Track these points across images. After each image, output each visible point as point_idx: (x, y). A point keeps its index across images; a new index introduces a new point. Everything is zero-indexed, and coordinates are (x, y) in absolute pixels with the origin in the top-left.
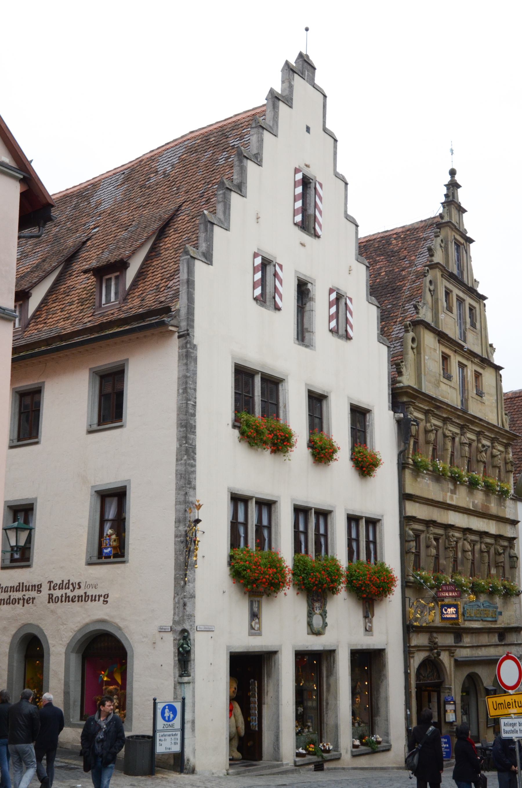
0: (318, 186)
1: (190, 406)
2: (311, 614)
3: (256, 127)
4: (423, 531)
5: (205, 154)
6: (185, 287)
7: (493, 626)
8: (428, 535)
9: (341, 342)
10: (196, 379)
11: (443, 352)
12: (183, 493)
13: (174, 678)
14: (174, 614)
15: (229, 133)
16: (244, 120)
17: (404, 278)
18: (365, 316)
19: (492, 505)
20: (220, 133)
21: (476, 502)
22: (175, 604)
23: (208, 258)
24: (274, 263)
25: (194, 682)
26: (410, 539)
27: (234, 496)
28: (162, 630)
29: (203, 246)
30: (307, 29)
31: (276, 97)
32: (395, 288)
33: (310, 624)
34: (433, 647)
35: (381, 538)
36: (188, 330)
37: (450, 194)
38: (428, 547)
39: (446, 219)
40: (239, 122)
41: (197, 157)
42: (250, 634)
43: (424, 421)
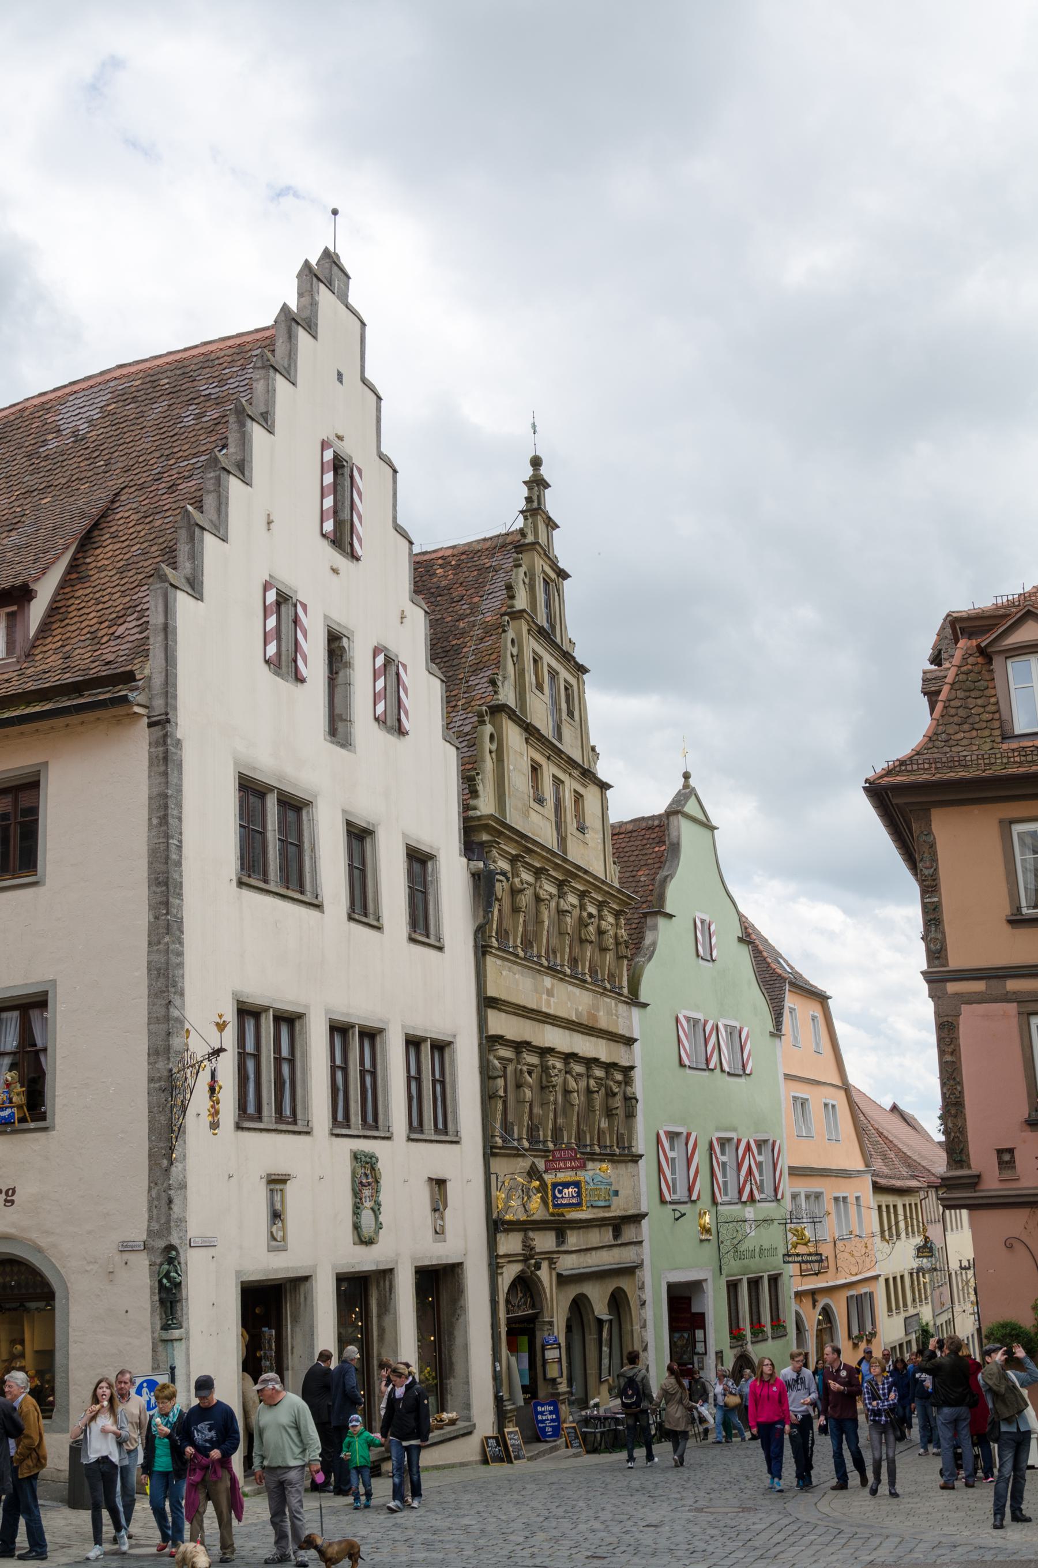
0: (356, 473)
1: (173, 848)
2: (358, 1208)
3: (263, 368)
4: (510, 1060)
5: (154, 406)
6: (160, 638)
7: (607, 1215)
8: (519, 1067)
9: (392, 739)
10: (181, 800)
11: (532, 760)
12: (164, 1002)
13: (153, 1332)
14: (150, 1218)
15: (196, 374)
16: (223, 353)
17: (463, 633)
18: (424, 693)
19: (601, 1013)
20: (178, 372)
21: (580, 1008)
23: (195, 587)
24: (294, 600)
25: (188, 1338)
26: (496, 1074)
28: (126, 1248)
29: (186, 567)
31: (294, 319)
32: (448, 649)
33: (356, 1227)
34: (528, 1255)
35: (453, 1074)
36: (167, 714)
37: (535, 498)
39: (530, 538)
40: (213, 356)
41: (138, 410)
42: (270, 1250)
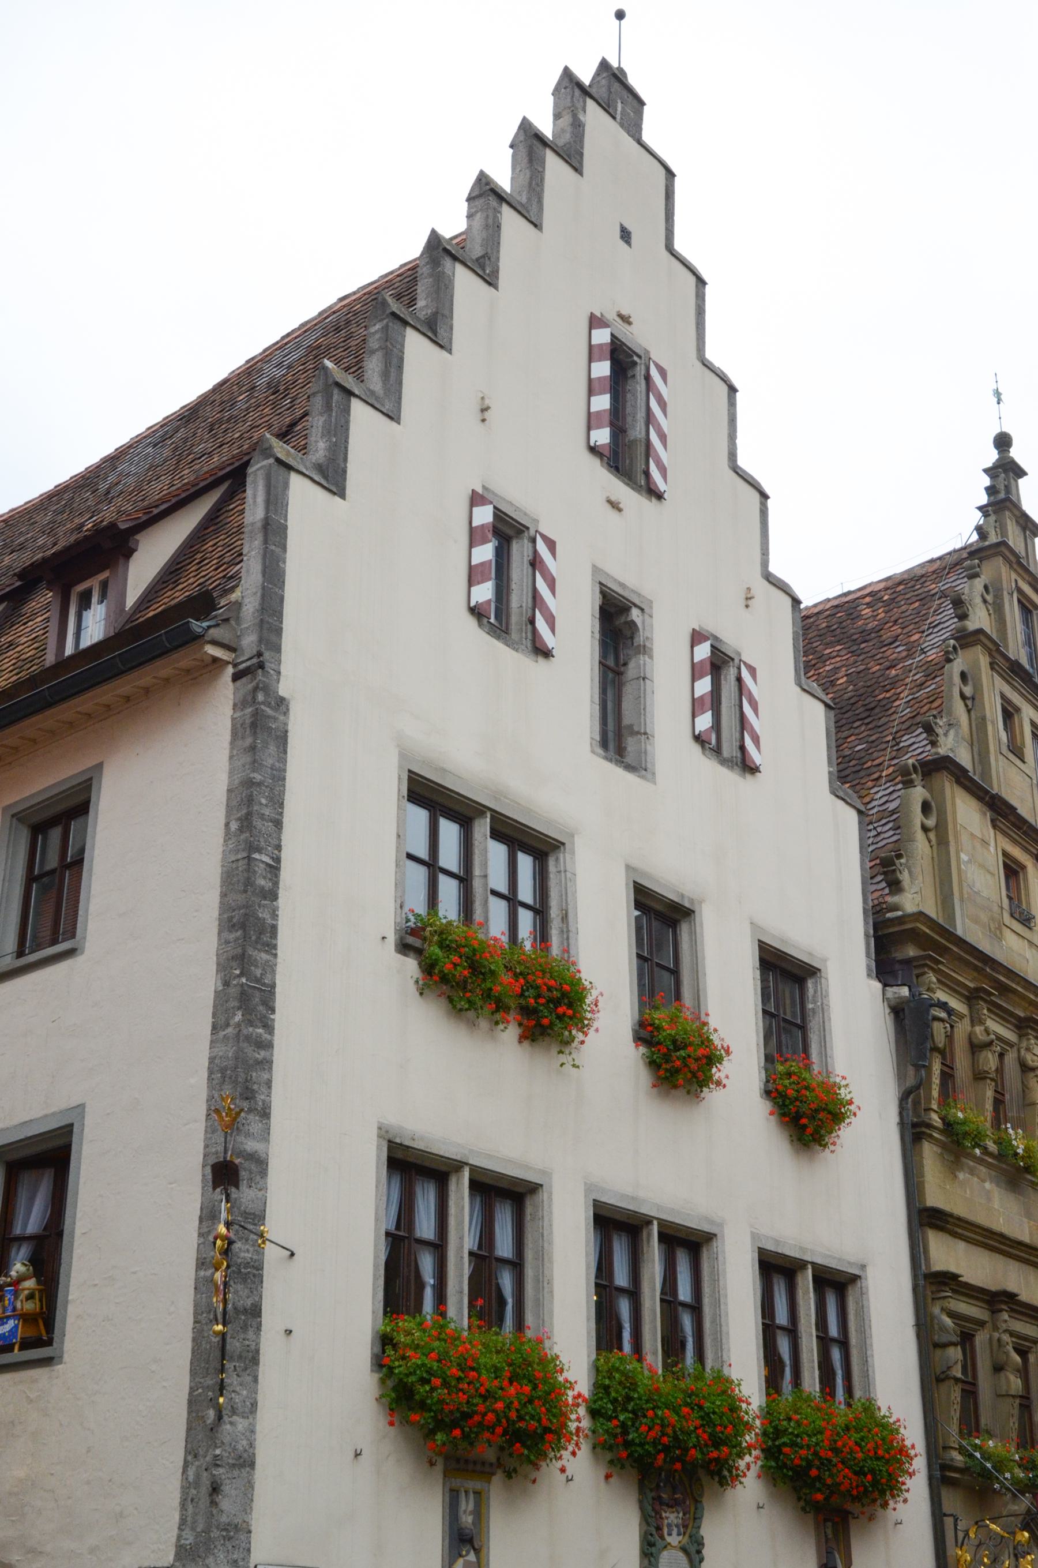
0: (654, 372)
2: (651, 1545)
4: (982, 1324)
8: (996, 1335)
9: (730, 777)
10: (283, 793)
11: (1005, 854)
14: (183, 1522)
17: (894, 683)
22: (185, 1489)
23: (333, 478)
24: (532, 532)
26: (944, 1339)
27: (399, 1155)
29: (320, 449)
30: (620, 15)
32: (872, 705)
36: (259, 654)
38: (998, 1368)
39: (993, 539)
43: (967, 1021)
